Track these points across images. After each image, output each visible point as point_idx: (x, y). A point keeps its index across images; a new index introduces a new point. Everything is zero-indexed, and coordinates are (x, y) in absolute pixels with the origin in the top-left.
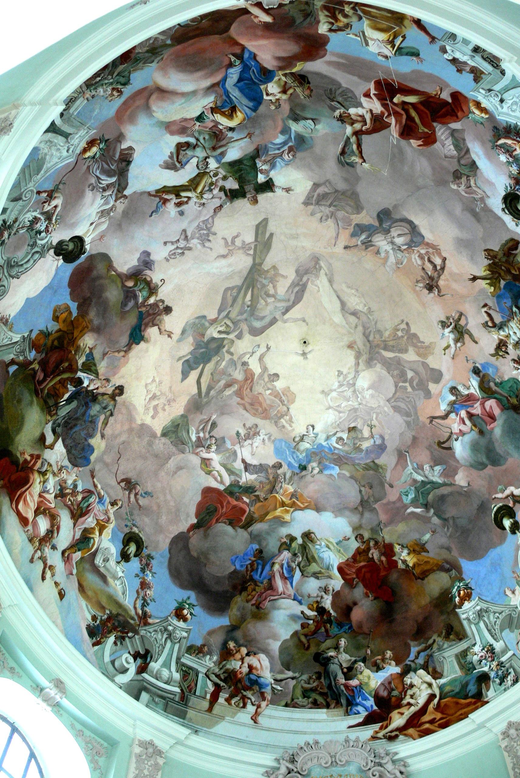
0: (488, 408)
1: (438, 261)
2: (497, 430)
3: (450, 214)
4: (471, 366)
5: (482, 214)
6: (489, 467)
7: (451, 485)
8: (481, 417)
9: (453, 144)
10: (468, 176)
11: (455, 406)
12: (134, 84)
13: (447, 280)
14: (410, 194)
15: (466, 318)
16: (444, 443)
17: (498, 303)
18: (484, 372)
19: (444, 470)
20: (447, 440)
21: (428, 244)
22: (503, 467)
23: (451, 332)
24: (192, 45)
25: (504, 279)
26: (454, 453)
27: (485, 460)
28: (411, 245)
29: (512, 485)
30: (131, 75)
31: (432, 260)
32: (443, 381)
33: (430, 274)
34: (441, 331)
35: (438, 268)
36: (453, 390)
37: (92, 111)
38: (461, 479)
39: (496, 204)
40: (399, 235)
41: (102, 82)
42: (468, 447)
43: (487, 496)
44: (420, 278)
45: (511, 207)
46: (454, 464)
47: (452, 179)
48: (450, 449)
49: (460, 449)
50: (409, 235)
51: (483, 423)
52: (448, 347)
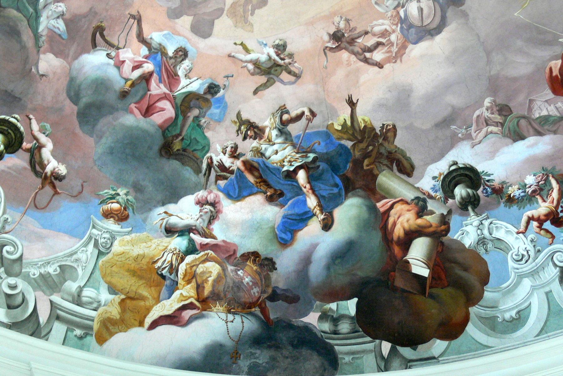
0: (160, 104)
1: (377, 56)
2: (132, 119)
3: (448, 86)
4: (220, 81)
5: (448, 133)
6: (75, 108)
7: (38, 47)
8: (146, 94)
9: (549, 116)
10: (502, 125)
11: (159, 54)
13: (349, 64)
14: (482, 40)
15: (293, 83)
16: (103, 36)
17: (318, 133)
18: (212, 100)
19: (60, 35)
20: (107, 42)
21: (403, 48)
22: (78, 130)
23: (270, 58)
25: (354, 145)
26: (88, 52)
27: (84, 100)
28: (405, 23)
29: (55, 145)
31: (380, 48)
32: (195, 39)
33: (359, 40)
34: (270, 43)
35: (368, 55)
36: (182, 53)
38: (48, 63)
39: (464, 155)
40: (421, 10)
42: (99, 74)
43: (30, 106)
44: (352, 25)
45: (461, 175)
46: (71, 53)
47: (499, 101)
48: (94, 45)
49: (95, 62)
50: (420, 24)
51: (138, 98)
52: (247, 50)
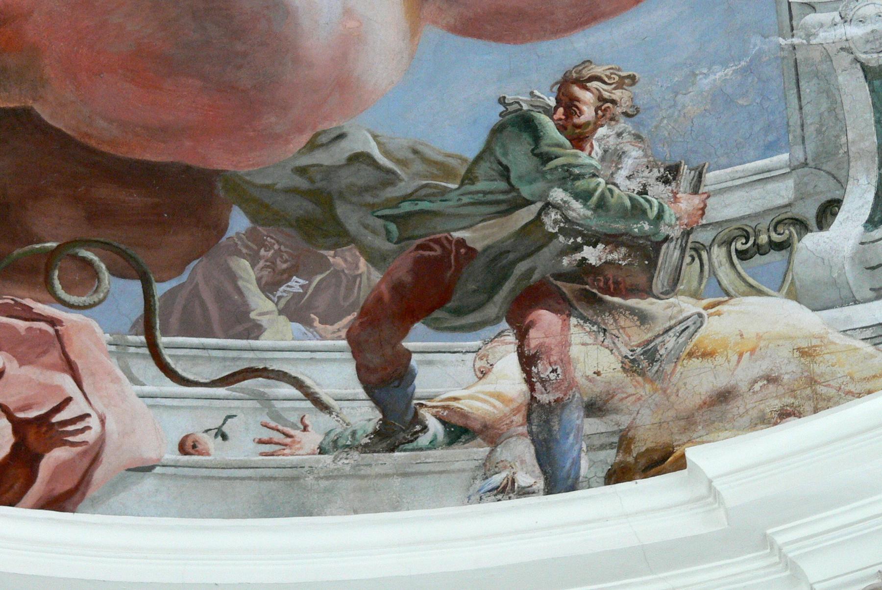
12: (493, 92)
24: (163, 132)
30: (471, 156)
37: (722, 99)
41: (597, 224)
